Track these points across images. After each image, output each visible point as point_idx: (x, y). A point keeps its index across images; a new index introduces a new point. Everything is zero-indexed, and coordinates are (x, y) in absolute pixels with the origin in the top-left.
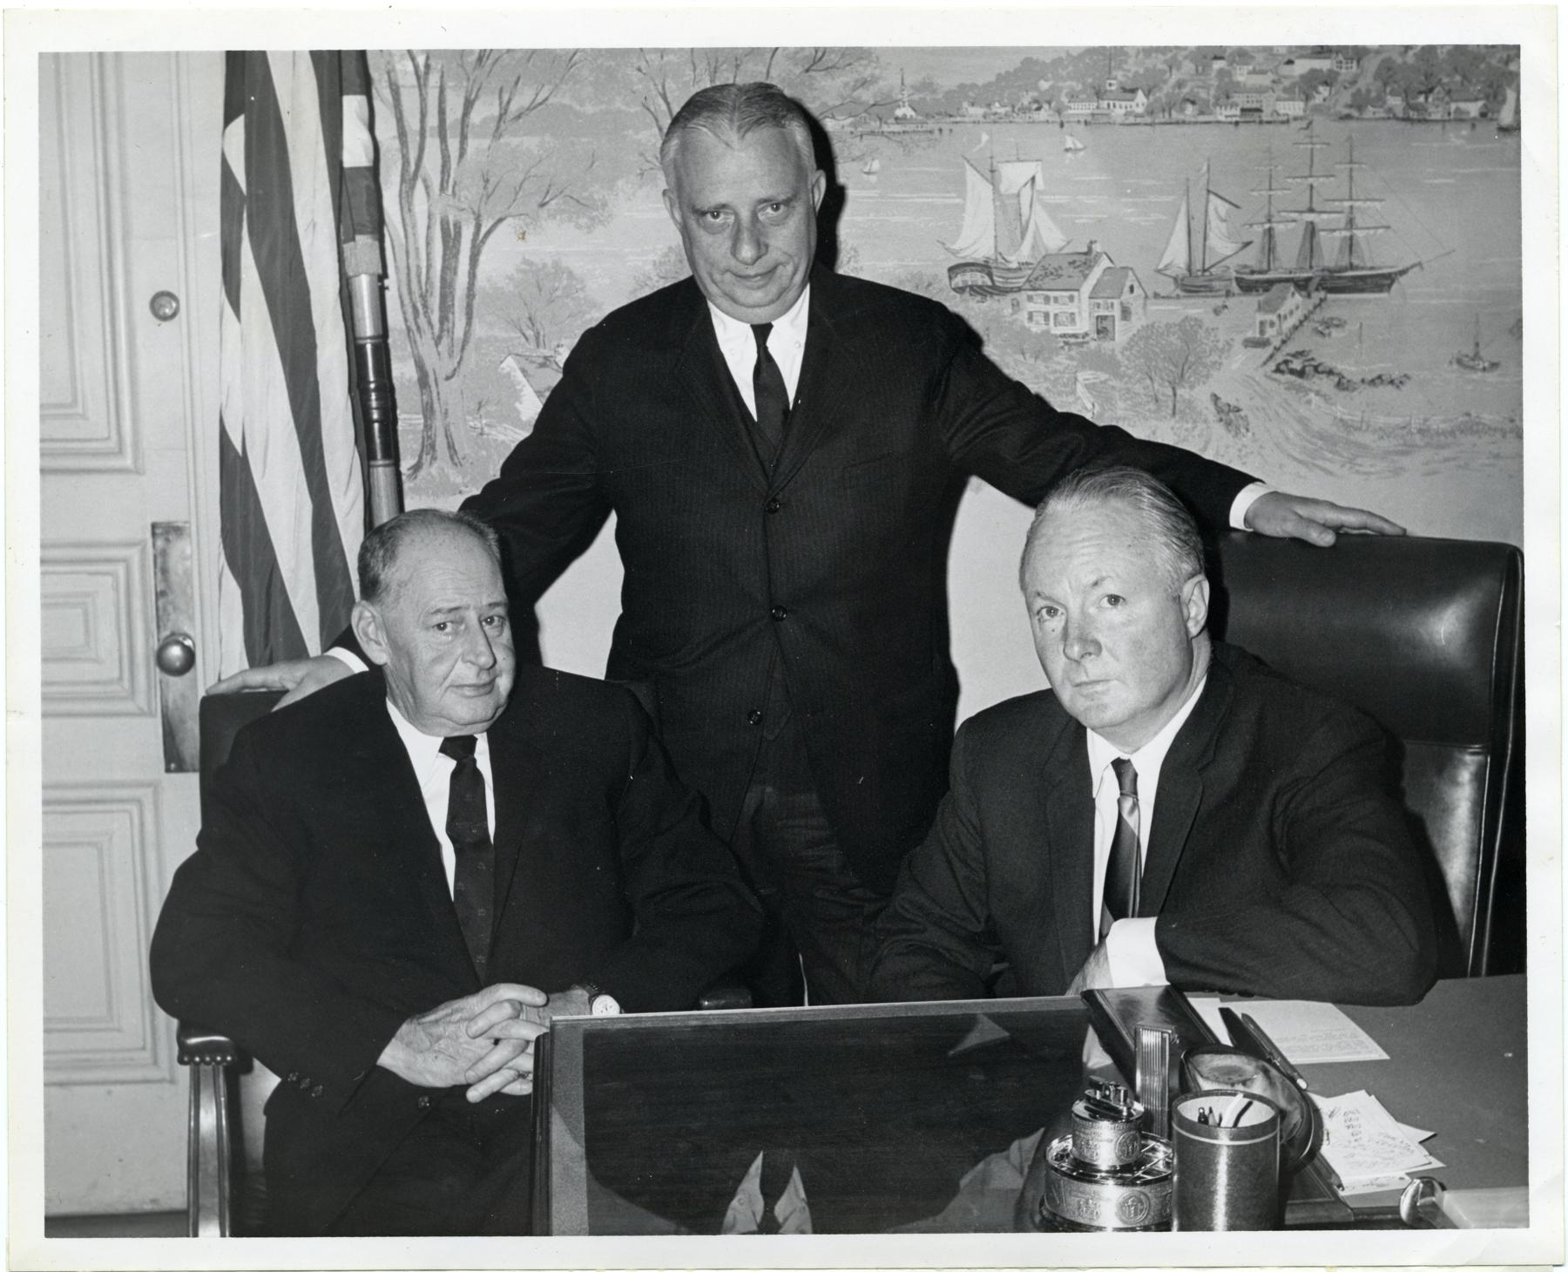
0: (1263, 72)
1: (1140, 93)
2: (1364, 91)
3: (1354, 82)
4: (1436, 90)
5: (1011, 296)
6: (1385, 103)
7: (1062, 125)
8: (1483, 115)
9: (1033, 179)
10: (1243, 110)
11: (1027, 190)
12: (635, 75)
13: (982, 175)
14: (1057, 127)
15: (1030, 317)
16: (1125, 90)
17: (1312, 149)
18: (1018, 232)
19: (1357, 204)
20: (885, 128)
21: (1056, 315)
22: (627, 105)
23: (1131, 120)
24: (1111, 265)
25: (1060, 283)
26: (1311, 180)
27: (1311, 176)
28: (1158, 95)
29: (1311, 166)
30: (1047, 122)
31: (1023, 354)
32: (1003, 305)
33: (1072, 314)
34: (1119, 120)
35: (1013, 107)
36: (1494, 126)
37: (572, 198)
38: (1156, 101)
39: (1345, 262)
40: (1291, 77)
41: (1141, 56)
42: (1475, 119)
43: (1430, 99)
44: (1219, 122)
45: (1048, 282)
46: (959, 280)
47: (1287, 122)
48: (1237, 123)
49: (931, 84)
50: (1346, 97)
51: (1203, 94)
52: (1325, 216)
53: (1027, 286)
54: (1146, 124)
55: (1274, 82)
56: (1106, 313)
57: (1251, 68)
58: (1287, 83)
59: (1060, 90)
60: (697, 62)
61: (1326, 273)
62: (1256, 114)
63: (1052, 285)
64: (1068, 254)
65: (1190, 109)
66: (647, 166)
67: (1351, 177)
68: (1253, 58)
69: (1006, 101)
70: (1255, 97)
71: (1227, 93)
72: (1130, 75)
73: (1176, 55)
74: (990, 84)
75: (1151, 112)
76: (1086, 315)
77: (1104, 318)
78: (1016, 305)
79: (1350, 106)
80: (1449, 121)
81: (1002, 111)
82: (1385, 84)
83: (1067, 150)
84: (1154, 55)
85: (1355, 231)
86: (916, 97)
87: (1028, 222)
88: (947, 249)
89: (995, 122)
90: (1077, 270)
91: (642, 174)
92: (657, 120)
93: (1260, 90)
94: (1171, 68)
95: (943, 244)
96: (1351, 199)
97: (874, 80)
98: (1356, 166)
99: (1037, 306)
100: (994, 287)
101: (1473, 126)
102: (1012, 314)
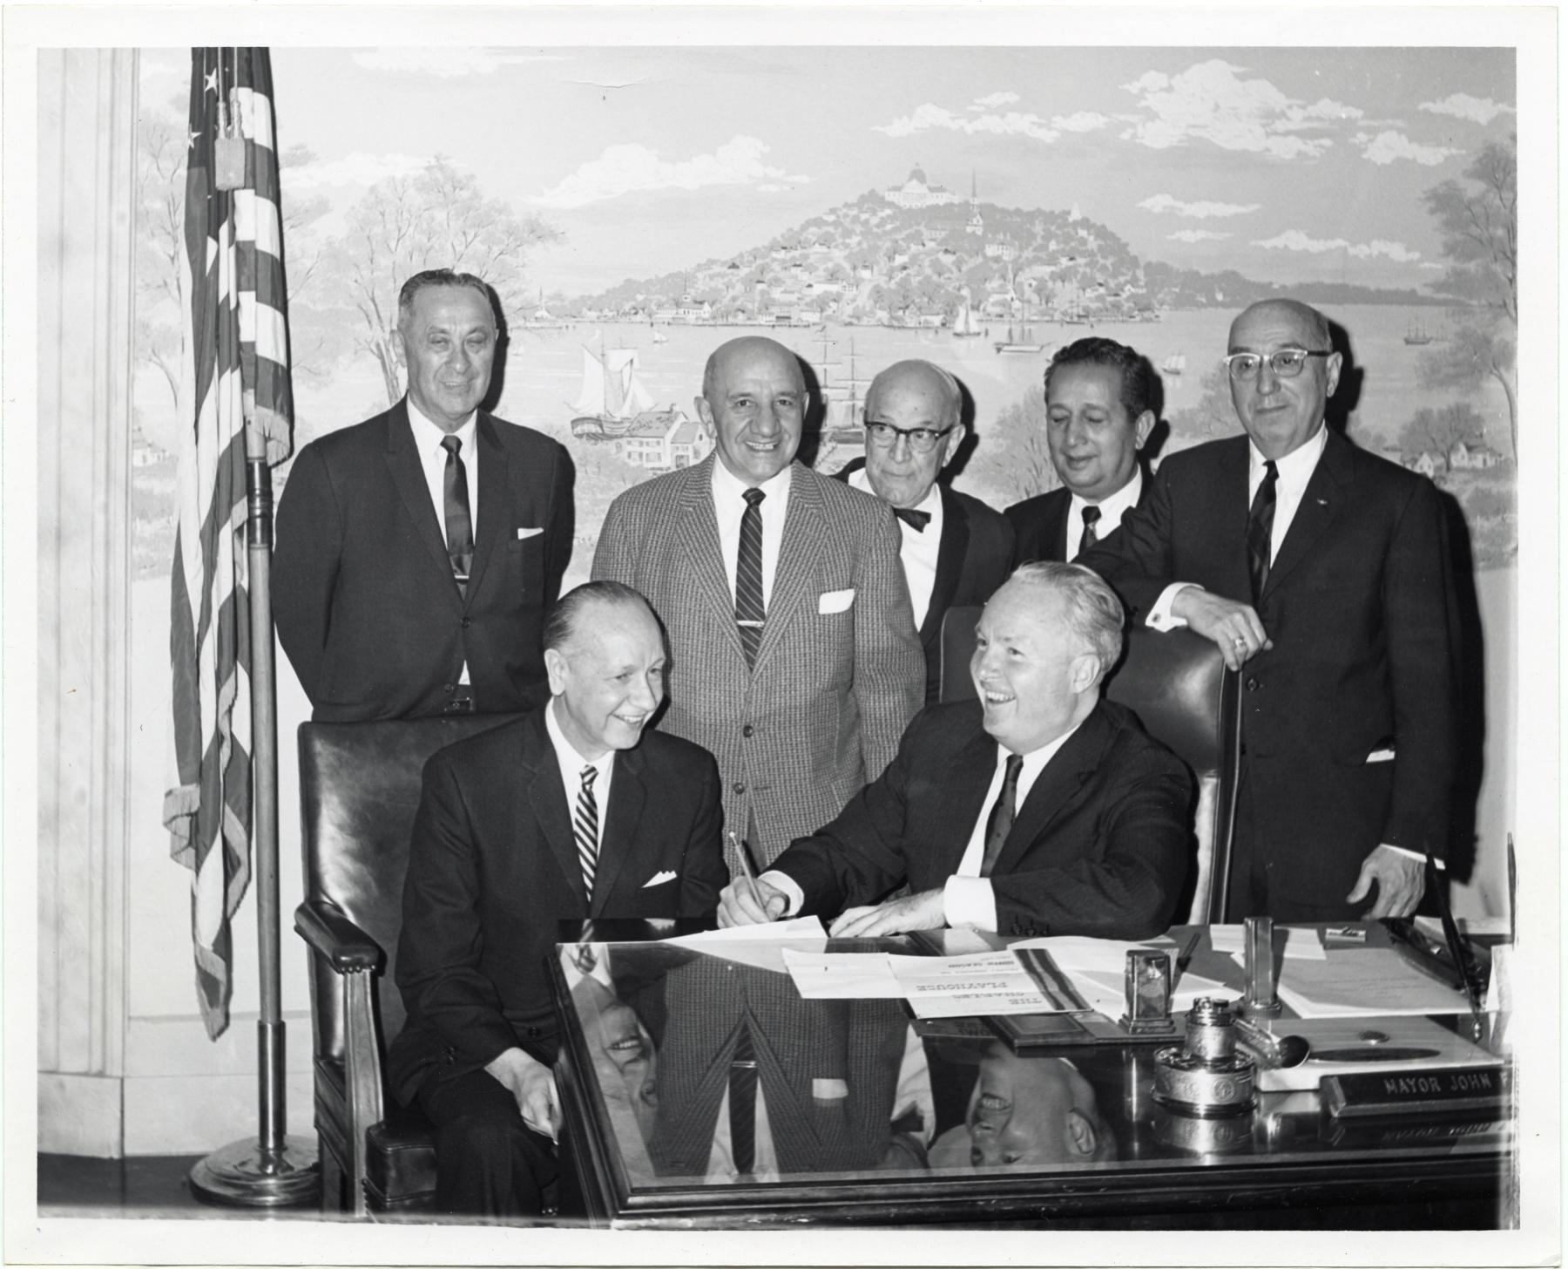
0: (792, 292)
1: (706, 304)
2: (861, 305)
3: (854, 300)
4: (912, 306)
5: (616, 441)
6: (875, 314)
7: (652, 325)
8: (943, 325)
9: (632, 361)
10: (778, 318)
11: (627, 370)
12: (353, 285)
13: (596, 357)
14: (649, 325)
15: (629, 455)
16: (696, 302)
17: (826, 346)
18: (621, 399)
19: (857, 383)
20: (528, 324)
21: (647, 455)
22: (347, 305)
23: (700, 322)
24: (685, 420)
25: (647, 433)
26: (824, 366)
27: (825, 363)
28: (719, 306)
29: (825, 357)
30: (642, 322)
31: (624, 480)
32: (611, 445)
33: (659, 454)
34: (693, 322)
35: (618, 312)
36: (949, 333)
37: (305, 368)
38: (718, 310)
39: (850, 423)
40: (810, 295)
41: (707, 279)
42: (938, 327)
43: (907, 312)
44: (760, 325)
45: (641, 432)
46: (579, 430)
47: (809, 326)
48: (773, 326)
49: (561, 295)
50: (849, 310)
51: (750, 306)
52: (834, 391)
53: (627, 434)
54: (710, 326)
55: (799, 299)
56: (680, 453)
57: (783, 289)
58: (808, 300)
59: (651, 301)
60: (397, 276)
61: (836, 430)
62: (786, 322)
63: (647, 433)
64: (656, 413)
65: (741, 317)
66: (359, 347)
67: (853, 366)
68: (784, 282)
69: (612, 307)
70: (786, 309)
71: (766, 307)
72: (699, 292)
73: (730, 280)
74: (602, 296)
75: (714, 318)
76: (668, 453)
77: (682, 457)
78: (619, 447)
79: (852, 317)
80: (920, 328)
81: (611, 314)
82: (876, 302)
83: (656, 342)
84: (716, 279)
85: (856, 402)
86: (550, 304)
87: (627, 393)
88: (571, 408)
89: (605, 322)
90: (662, 425)
91: (356, 353)
92: (367, 316)
93: (790, 304)
94: (728, 287)
95: (568, 404)
96: (853, 379)
97: (521, 292)
98: (855, 357)
99: (634, 447)
100: (603, 434)
101: (937, 332)
102: (618, 452)
